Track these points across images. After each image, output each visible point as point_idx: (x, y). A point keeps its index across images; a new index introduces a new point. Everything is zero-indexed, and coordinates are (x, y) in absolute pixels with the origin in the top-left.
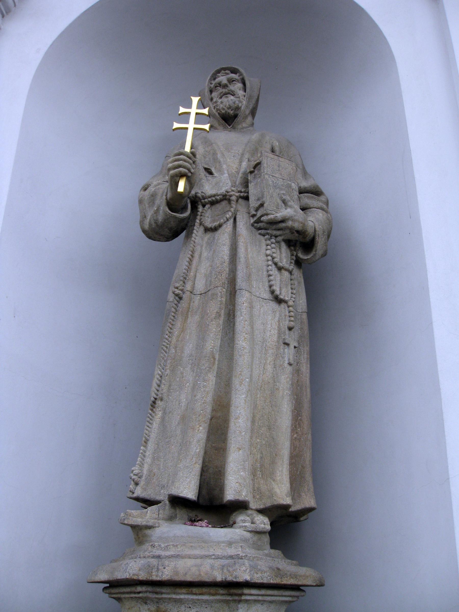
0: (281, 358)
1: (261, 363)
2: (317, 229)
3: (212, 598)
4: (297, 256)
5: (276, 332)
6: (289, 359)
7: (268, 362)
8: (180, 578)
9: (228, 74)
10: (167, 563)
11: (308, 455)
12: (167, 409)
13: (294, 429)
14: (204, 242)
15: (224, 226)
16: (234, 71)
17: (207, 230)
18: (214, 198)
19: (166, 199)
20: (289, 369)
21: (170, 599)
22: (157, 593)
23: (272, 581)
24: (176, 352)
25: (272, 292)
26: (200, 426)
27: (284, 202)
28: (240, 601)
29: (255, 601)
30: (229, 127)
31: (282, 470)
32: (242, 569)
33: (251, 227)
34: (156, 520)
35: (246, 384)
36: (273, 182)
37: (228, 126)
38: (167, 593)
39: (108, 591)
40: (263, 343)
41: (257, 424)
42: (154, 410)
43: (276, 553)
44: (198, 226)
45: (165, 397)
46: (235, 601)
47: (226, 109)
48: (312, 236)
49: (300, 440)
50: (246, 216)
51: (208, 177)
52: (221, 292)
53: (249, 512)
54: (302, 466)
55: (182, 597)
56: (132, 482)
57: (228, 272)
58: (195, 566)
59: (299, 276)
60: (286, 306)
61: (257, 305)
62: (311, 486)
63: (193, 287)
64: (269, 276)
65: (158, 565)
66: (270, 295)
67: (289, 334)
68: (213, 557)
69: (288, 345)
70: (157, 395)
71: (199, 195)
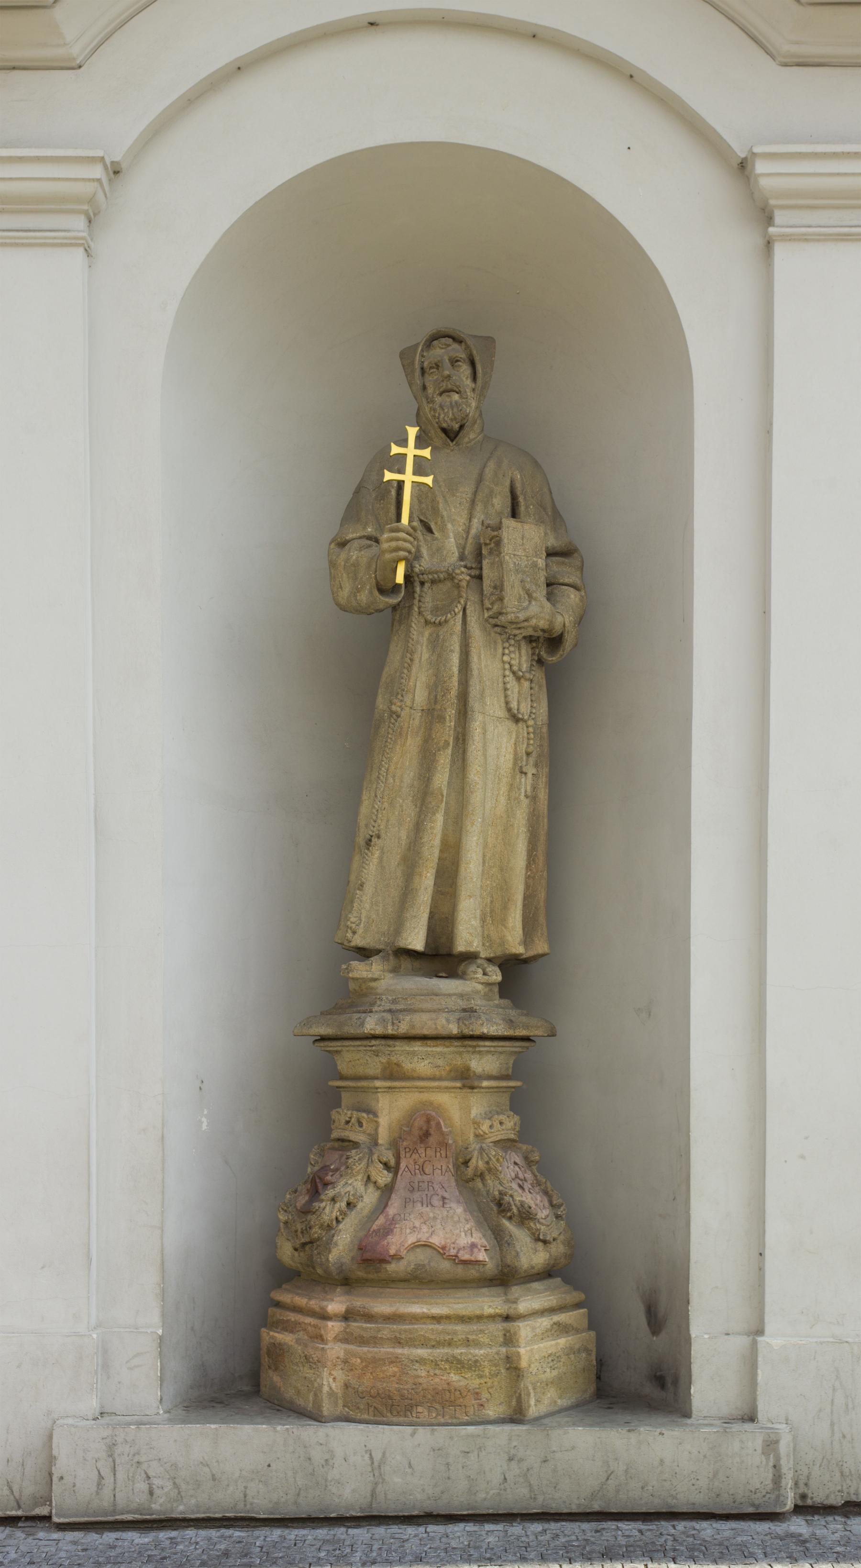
0: (516, 789)
4: (539, 655)
5: (512, 756)
6: (526, 791)
7: (502, 792)
10: (401, 1017)
11: (542, 895)
12: (385, 848)
13: (528, 867)
14: (425, 639)
18: (436, 576)
20: (525, 802)
23: (506, 1033)
24: (394, 781)
25: (509, 710)
30: (451, 444)
31: (515, 917)
32: (479, 1023)
34: (381, 972)
35: (479, 825)
37: (450, 442)
40: (496, 771)
41: (487, 865)
43: (505, 1002)
44: (417, 617)
45: (383, 835)
47: (449, 422)
48: (560, 633)
49: (534, 878)
51: (426, 535)
53: (479, 961)
54: (536, 908)
57: (457, 688)
58: (431, 1020)
59: (540, 678)
60: (525, 726)
61: (490, 728)
62: (545, 929)
63: (413, 700)
64: (504, 676)
65: (392, 1019)
66: (507, 713)
67: (527, 761)
68: (446, 1010)
69: (526, 774)
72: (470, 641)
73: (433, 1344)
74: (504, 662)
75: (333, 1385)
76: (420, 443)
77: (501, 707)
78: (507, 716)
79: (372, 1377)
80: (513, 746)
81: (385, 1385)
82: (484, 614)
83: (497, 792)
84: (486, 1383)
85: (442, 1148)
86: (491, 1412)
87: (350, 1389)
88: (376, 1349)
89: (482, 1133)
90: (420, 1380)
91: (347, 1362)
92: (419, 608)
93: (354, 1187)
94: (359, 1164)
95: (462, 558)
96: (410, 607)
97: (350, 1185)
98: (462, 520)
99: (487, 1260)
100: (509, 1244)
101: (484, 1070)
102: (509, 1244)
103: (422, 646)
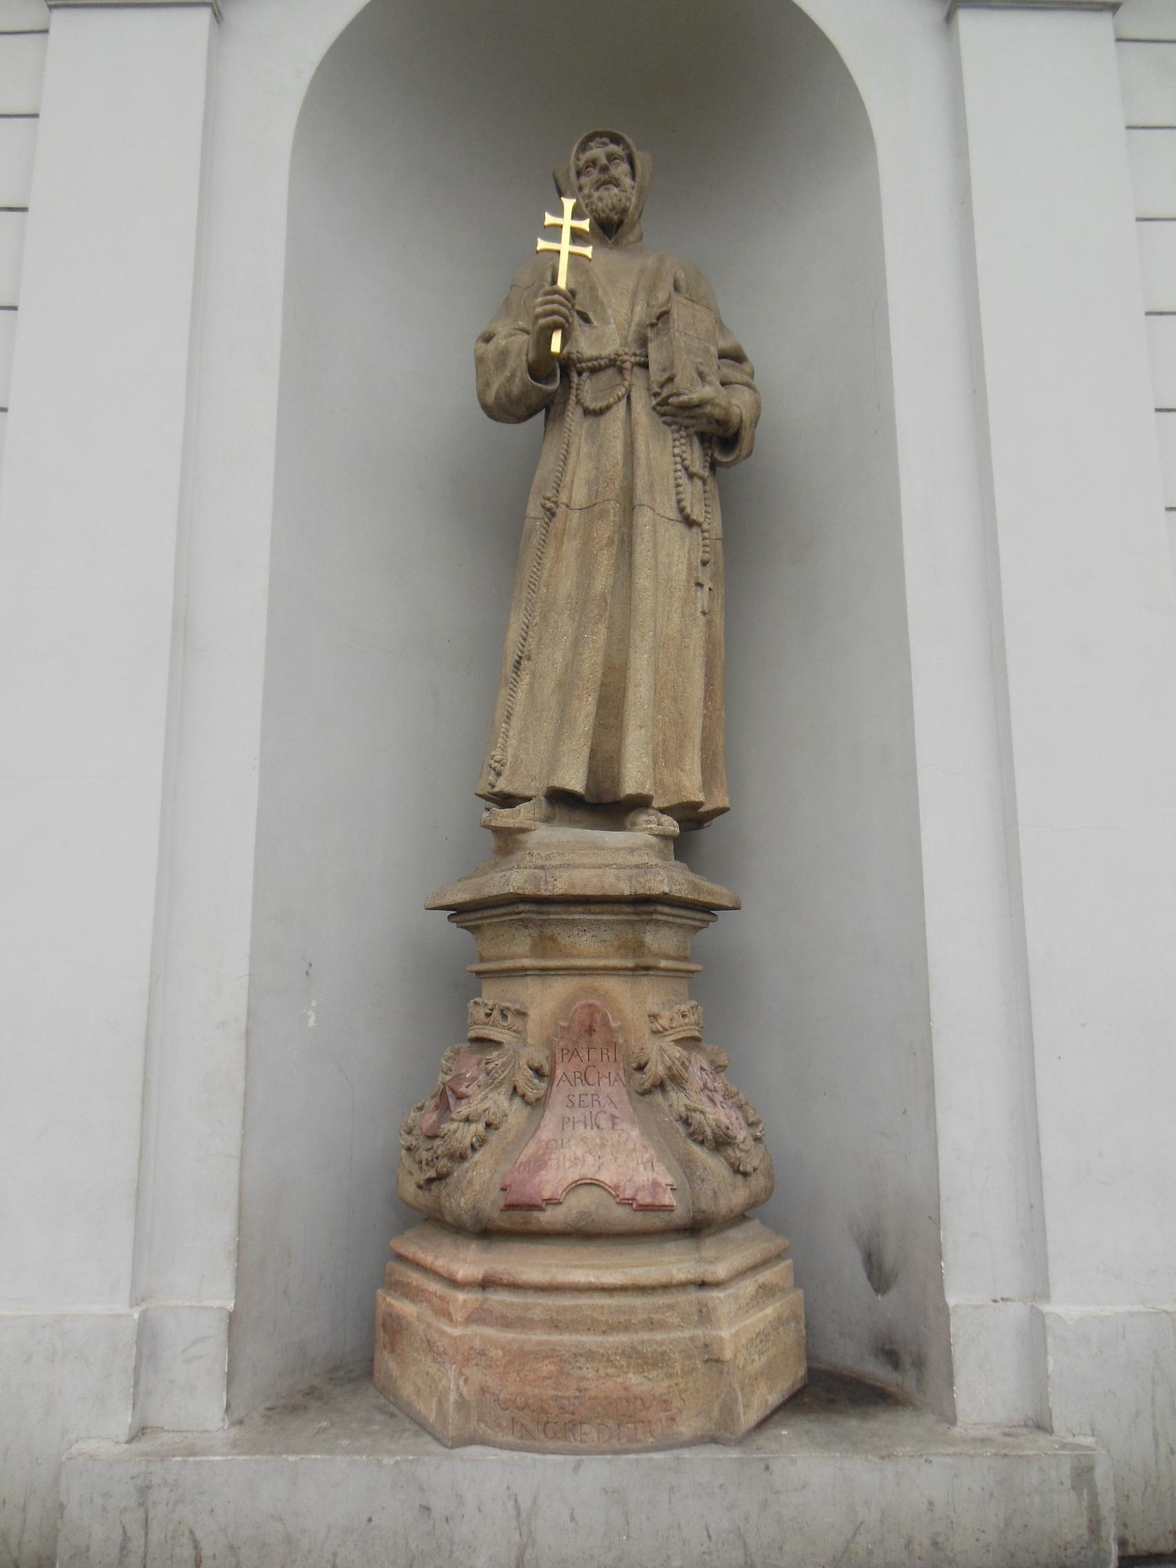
0: (692, 605)
1: (664, 609)
2: (744, 418)
3: (613, 917)
4: (712, 457)
5: (685, 567)
6: (703, 606)
7: (674, 609)
8: (578, 891)
9: (605, 144)
10: (557, 873)
12: (536, 672)
14: (584, 431)
15: (615, 408)
16: (616, 139)
17: (587, 412)
18: (596, 363)
19: (527, 360)
20: (702, 620)
21: (558, 920)
22: (542, 913)
24: (548, 592)
26: (589, 695)
27: (702, 376)
28: (649, 922)
29: (667, 923)
30: (610, 242)
31: (693, 757)
33: (651, 411)
34: (532, 822)
35: (650, 639)
36: (686, 343)
37: (608, 240)
38: (557, 914)
39: (458, 919)
40: (667, 582)
42: (519, 673)
44: (574, 406)
45: (534, 656)
46: (642, 921)
47: (608, 211)
48: (736, 429)
50: (644, 393)
51: (584, 326)
52: (614, 509)
53: (651, 811)
54: (714, 753)
55: (576, 917)
56: (493, 772)
58: (596, 877)
60: (699, 530)
63: (570, 498)
65: (546, 876)
66: (679, 515)
68: (614, 866)
70: (522, 652)
71: (574, 356)
72: (636, 427)
73: (604, 1328)
74: (674, 456)
75: (464, 1390)
76: (577, 214)
77: (672, 507)
78: (679, 519)
79: (518, 1379)
80: (686, 555)
81: (536, 1391)
82: (651, 402)
83: (669, 608)
84: (677, 1384)
85: (610, 1050)
86: (686, 1427)
87: (488, 1396)
88: (523, 1337)
89: (661, 1029)
90: (585, 1384)
91: (485, 1354)
92: (577, 396)
93: (495, 1102)
94: (503, 1072)
95: (625, 344)
96: (567, 399)
97: (491, 1099)
98: (624, 310)
99: (675, 1204)
100: (703, 1181)
101: (660, 948)
102: (703, 1181)
103: (580, 439)
